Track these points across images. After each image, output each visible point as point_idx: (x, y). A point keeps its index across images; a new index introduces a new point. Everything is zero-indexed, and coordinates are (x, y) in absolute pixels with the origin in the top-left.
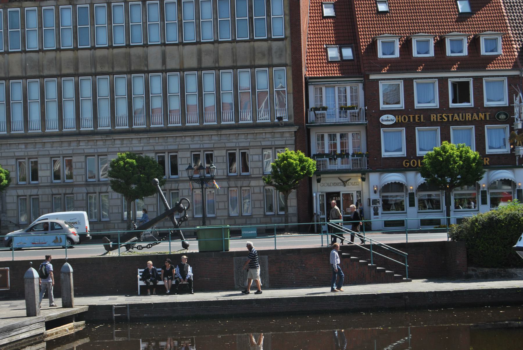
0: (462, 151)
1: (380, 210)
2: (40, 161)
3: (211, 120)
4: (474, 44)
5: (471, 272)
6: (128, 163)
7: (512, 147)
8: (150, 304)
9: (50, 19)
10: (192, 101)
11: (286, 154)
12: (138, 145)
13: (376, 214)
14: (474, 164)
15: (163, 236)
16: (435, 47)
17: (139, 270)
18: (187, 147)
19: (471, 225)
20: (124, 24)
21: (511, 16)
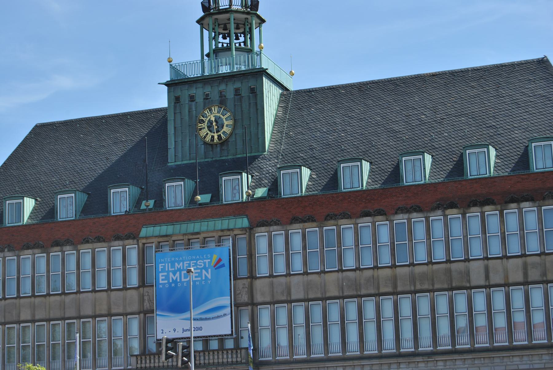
9: (366, 237)
10: (519, 318)
12: (462, 366)
20: (443, 239)
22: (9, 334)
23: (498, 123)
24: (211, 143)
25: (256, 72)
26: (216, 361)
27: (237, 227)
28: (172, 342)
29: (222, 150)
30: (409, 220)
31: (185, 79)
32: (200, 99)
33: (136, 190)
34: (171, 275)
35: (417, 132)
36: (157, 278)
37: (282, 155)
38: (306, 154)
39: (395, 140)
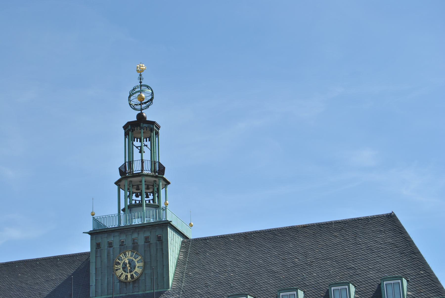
23: (356, 265)
24: (125, 281)
25: (162, 224)
31: (105, 229)
32: (116, 245)
35: (292, 273)
37: (183, 291)
38: (202, 290)
39: (274, 279)
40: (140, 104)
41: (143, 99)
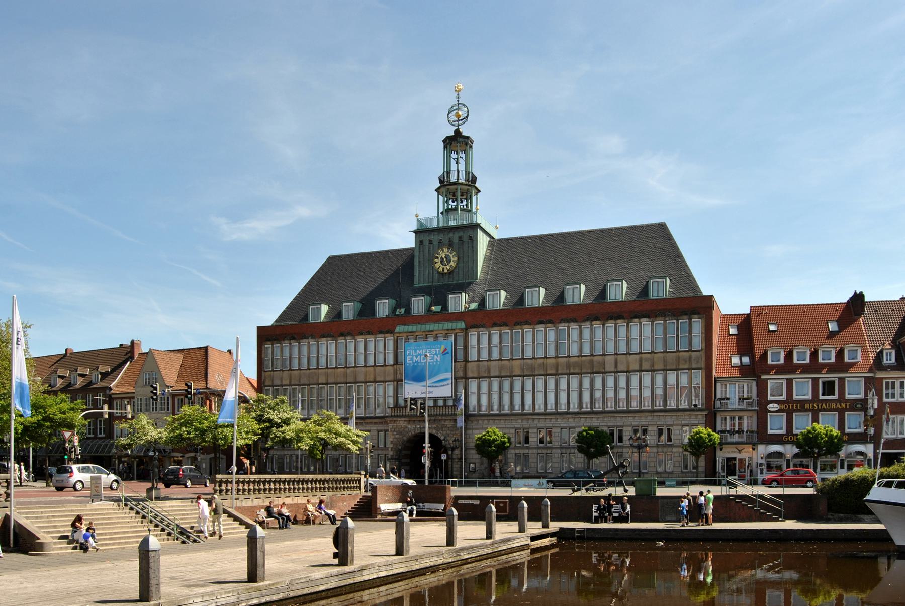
0: (827, 430)
1: (765, 471)
2: (530, 431)
3: (647, 405)
4: (840, 354)
5: (829, 517)
6: (589, 433)
7: (865, 428)
8: (601, 529)
10: (634, 393)
11: (699, 430)
13: (762, 473)
14: (836, 440)
15: (611, 484)
16: (810, 356)
17: (594, 506)
18: (629, 424)
19: (832, 484)
21: (869, 333)
22: (311, 391)
26: (441, 413)
27: (457, 328)
28: (414, 401)
29: (449, 277)
30: (568, 327)
33: (393, 302)
34: (414, 357)
36: (405, 359)
40: (457, 121)
41: (460, 116)
